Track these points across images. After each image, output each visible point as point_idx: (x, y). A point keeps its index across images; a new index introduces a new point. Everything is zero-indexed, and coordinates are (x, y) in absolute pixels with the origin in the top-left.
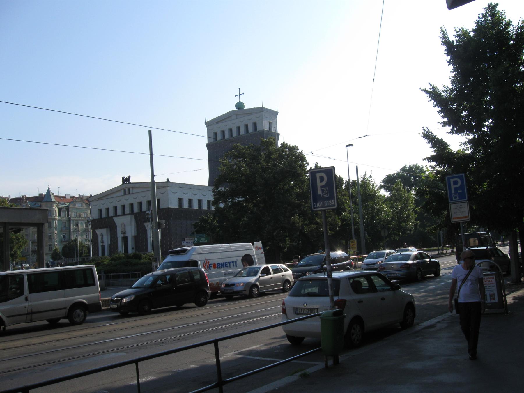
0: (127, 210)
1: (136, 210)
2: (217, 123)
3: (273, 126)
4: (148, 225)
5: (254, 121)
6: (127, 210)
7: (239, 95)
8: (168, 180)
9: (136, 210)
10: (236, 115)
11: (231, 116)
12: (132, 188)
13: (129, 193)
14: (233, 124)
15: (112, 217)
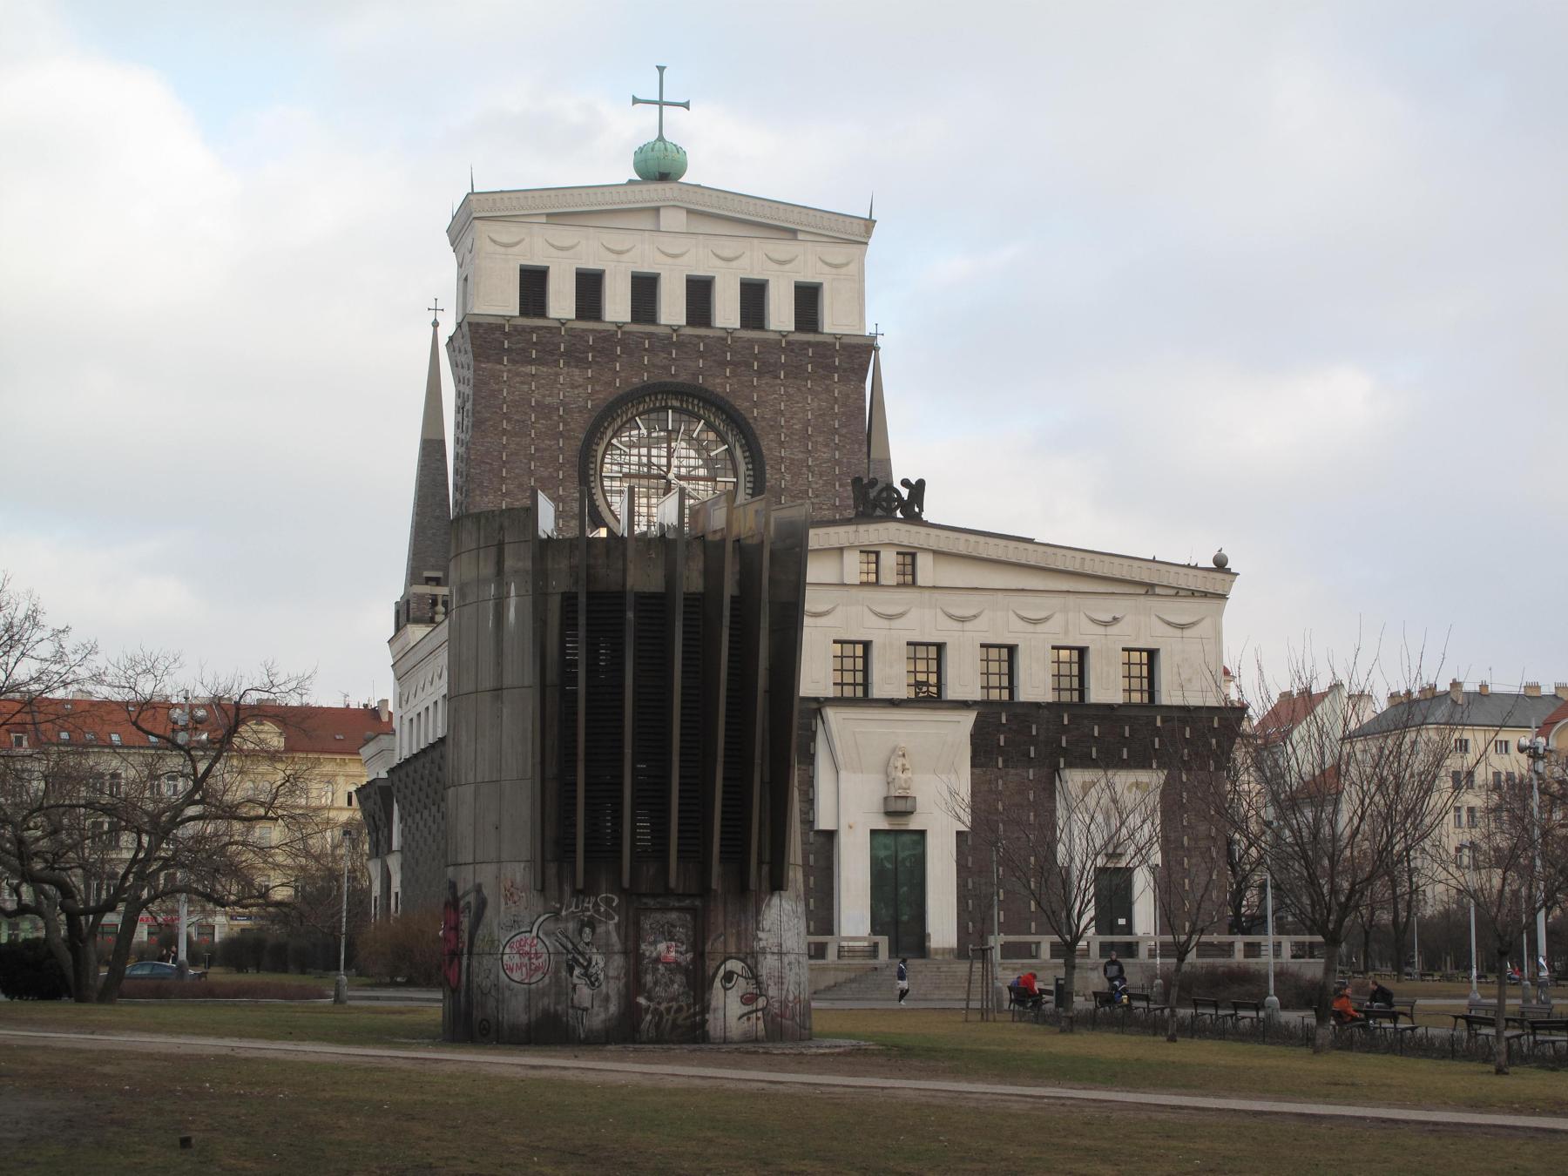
0: (891, 678)
1: (965, 680)
4: (1086, 788)
5: (808, 277)
6: (891, 678)
8: (1220, 565)
9: (965, 680)
10: (690, 212)
11: (657, 210)
12: (935, 552)
13: (908, 580)
14: (675, 259)
15: (818, 705)
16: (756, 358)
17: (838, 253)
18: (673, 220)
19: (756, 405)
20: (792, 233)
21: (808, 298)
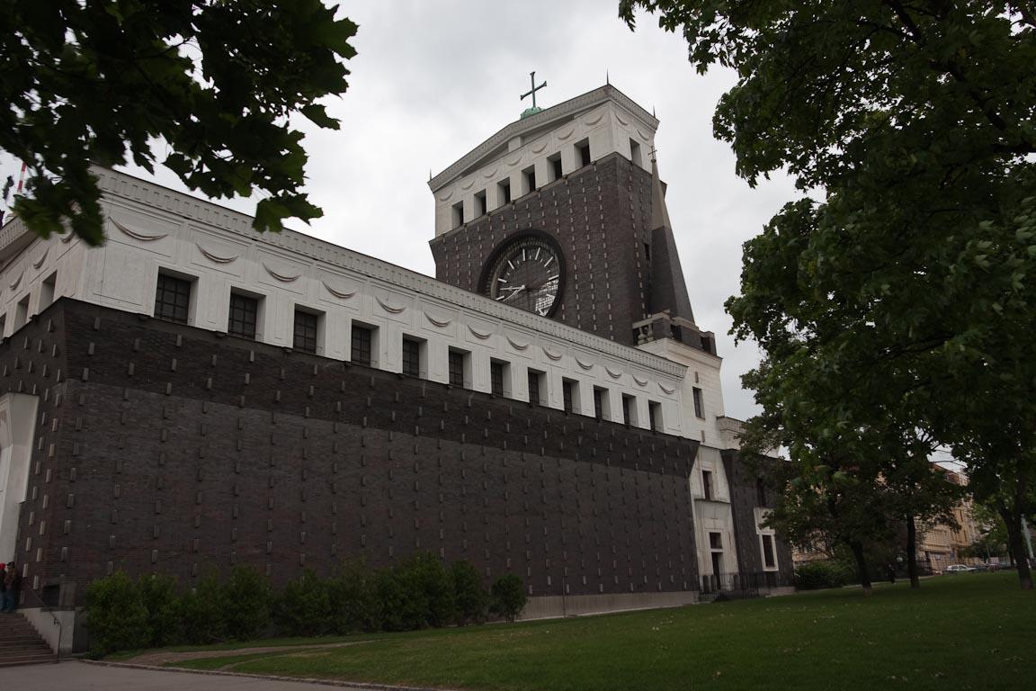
2: (465, 174)
3: (644, 150)
5: (580, 138)
7: (534, 90)
10: (523, 137)
16: (555, 198)
17: (592, 116)
18: (512, 146)
19: (559, 226)
20: (570, 118)
21: (583, 149)
